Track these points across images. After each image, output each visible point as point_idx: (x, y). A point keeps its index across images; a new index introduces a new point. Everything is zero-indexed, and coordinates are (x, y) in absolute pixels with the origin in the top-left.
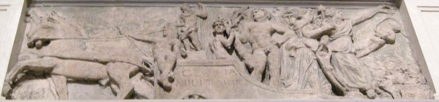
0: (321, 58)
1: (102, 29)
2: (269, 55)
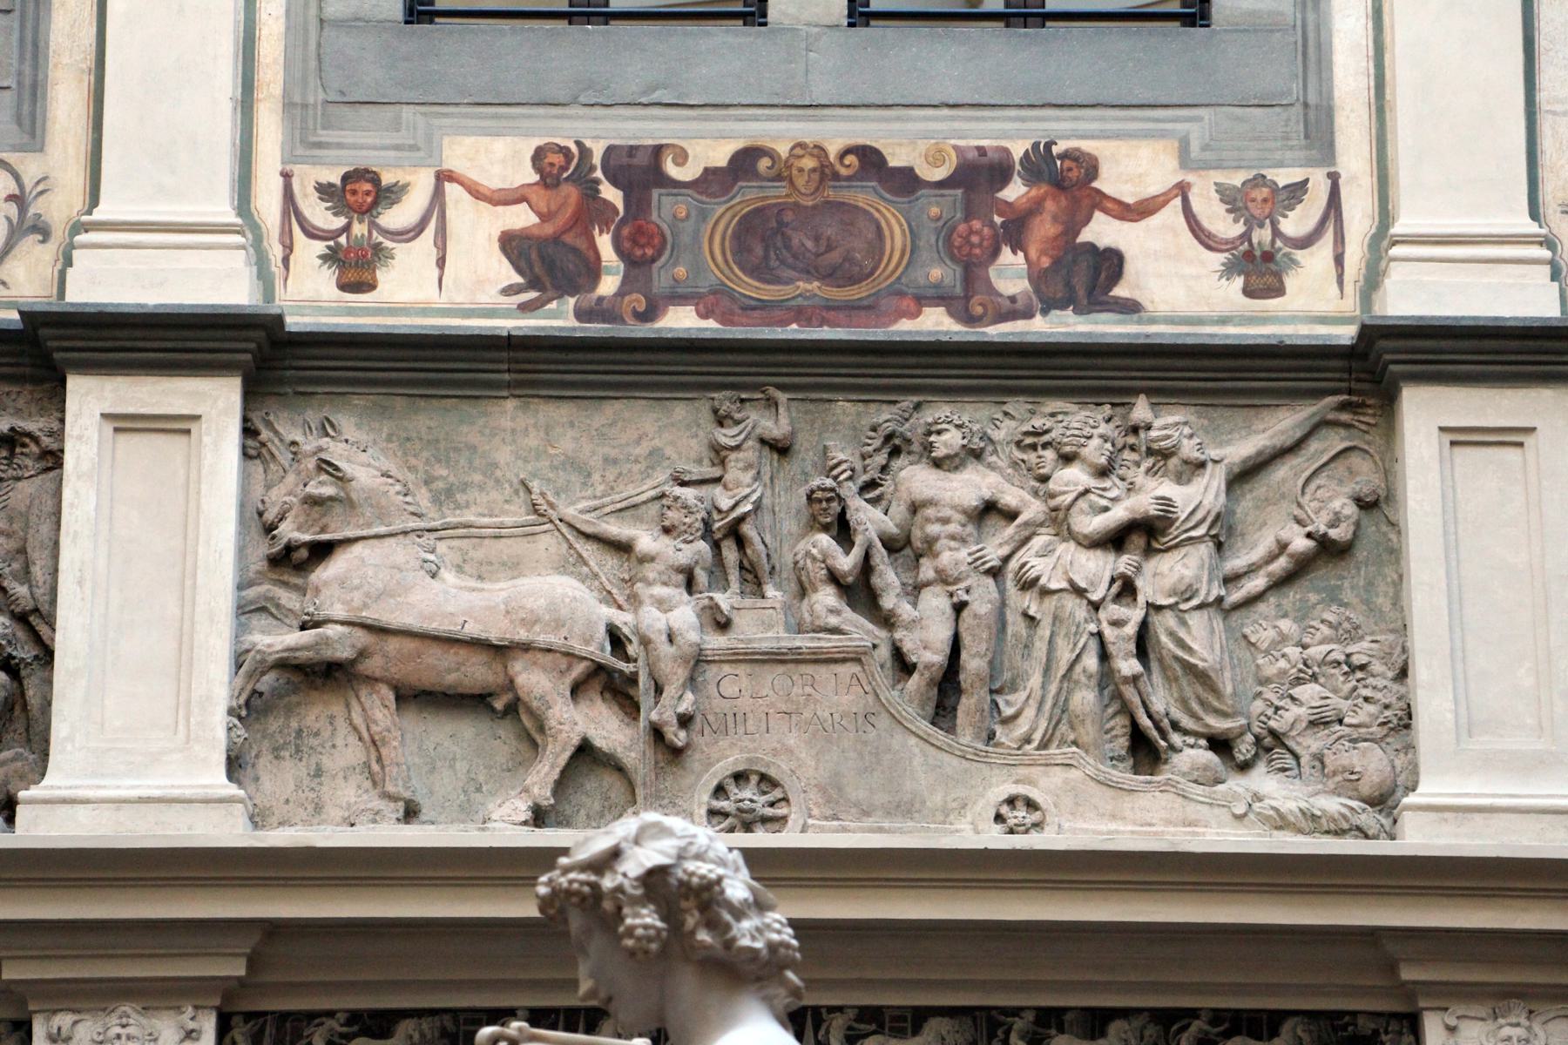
0: (1109, 633)
1: (481, 488)
2: (965, 614)
